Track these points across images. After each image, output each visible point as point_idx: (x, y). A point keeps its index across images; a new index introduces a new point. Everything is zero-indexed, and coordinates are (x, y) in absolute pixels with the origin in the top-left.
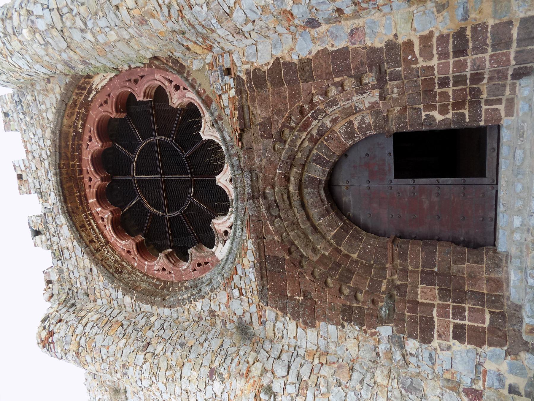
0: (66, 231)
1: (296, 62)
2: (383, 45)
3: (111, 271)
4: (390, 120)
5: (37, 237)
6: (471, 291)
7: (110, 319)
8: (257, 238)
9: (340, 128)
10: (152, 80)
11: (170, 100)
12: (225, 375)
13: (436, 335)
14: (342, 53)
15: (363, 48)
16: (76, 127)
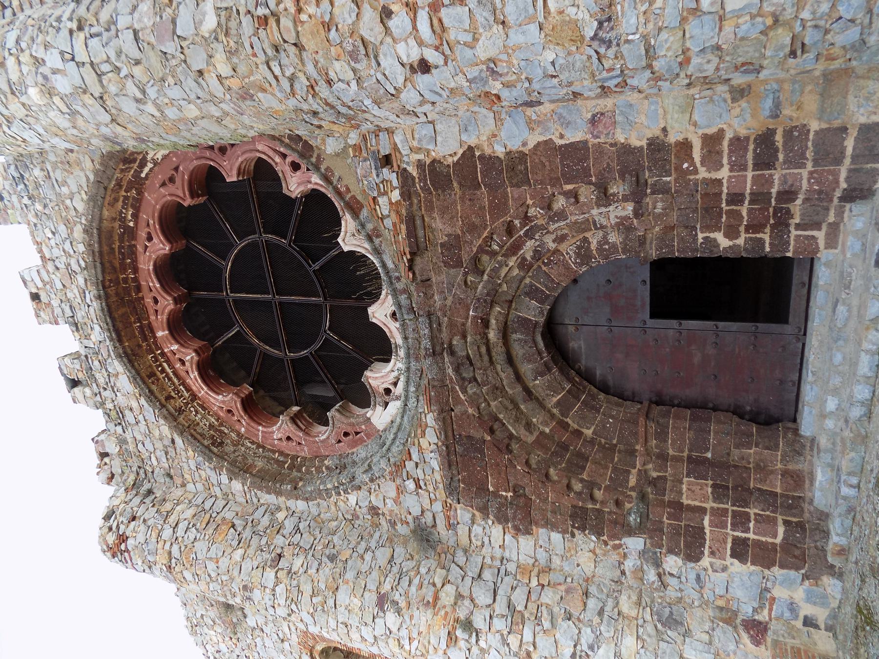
0: (124, 382)
1: (502, 156)
2: (644, 143)
3: (206, 443)
4: (648, 242)
5: (76, 390)
6: (759, 489)
7: (214, 515)
8: (441, 411)
9: (568, 249)
10: (251, 151)
11: (284, 185)
12: (403, 604)
13: (706, 552)
14: (577, 150)
15: (612, 145)
16: (123, 220)
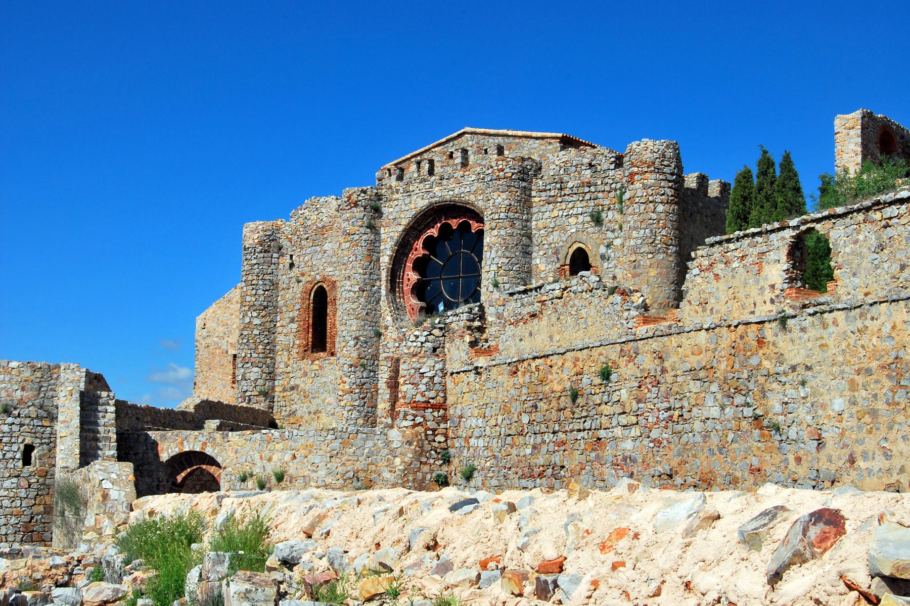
12: (358, 346)
